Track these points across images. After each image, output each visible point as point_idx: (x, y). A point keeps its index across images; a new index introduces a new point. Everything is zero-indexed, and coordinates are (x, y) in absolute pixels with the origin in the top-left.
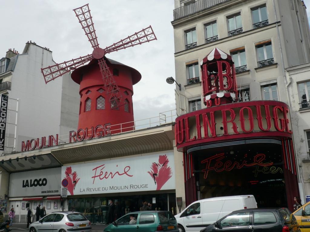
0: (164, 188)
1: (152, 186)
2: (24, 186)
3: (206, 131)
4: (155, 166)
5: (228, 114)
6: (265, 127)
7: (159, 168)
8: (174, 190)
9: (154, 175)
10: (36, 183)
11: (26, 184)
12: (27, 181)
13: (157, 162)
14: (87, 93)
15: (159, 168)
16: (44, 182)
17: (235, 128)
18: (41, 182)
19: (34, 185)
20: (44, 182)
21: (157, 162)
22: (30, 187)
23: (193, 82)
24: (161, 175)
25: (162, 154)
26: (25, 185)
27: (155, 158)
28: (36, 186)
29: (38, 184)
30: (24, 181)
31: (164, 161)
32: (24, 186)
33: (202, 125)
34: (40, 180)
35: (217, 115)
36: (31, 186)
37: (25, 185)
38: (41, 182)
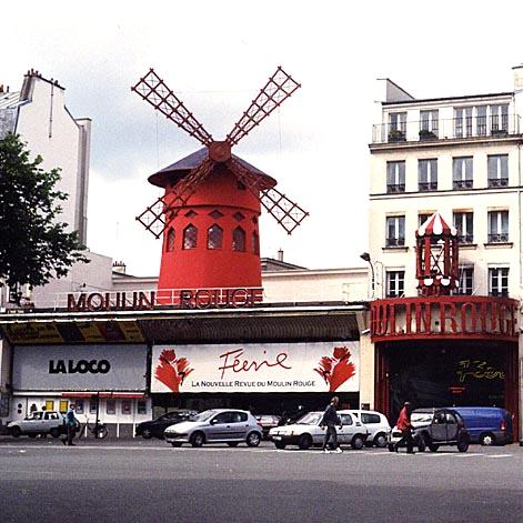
0: (343, 388)
1: (322, 386)
2: (52, 371)
3: (418, 325)
4: (326, 362)
5: (448, 307)
6: (489, 328)
7: (334, 364)
8: (358, 393)
9: (324, 374)
10: (83, 367)
11: (58, 367)
12: (61, 363)
13: (331, 356)
14: (187, 215)
15: (334, 364)
16: (104, 367)
17: (454, 326)
18: (95, 367)
19: (78, 369)
20: (104, 367)
21: (331, 356)
22: (68, 375)
23: (394, 243)
24: (338, 370)
25: (340, 345)
26: (55, 368)
27: (327, 350)
28: (84, 371)
29: (89, 367)
30: (52, 363)
31: (342, 355)
32: (52, 371)
33: (414, 316)
34: (94, 362)
35: (434, 306)
36: (71, 371)
37: (55, 368)
38: (95, 367)
